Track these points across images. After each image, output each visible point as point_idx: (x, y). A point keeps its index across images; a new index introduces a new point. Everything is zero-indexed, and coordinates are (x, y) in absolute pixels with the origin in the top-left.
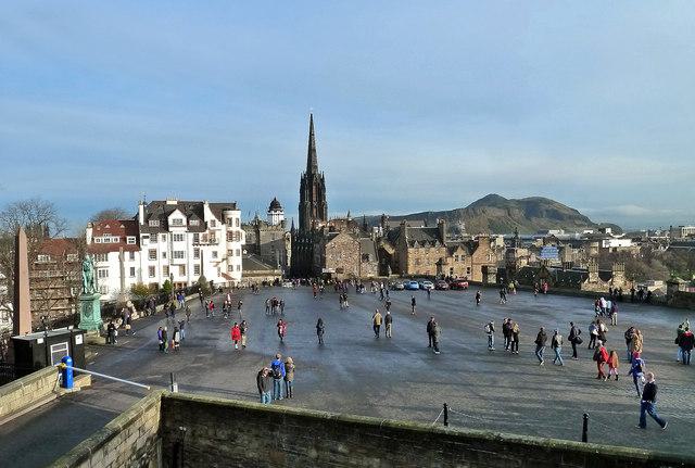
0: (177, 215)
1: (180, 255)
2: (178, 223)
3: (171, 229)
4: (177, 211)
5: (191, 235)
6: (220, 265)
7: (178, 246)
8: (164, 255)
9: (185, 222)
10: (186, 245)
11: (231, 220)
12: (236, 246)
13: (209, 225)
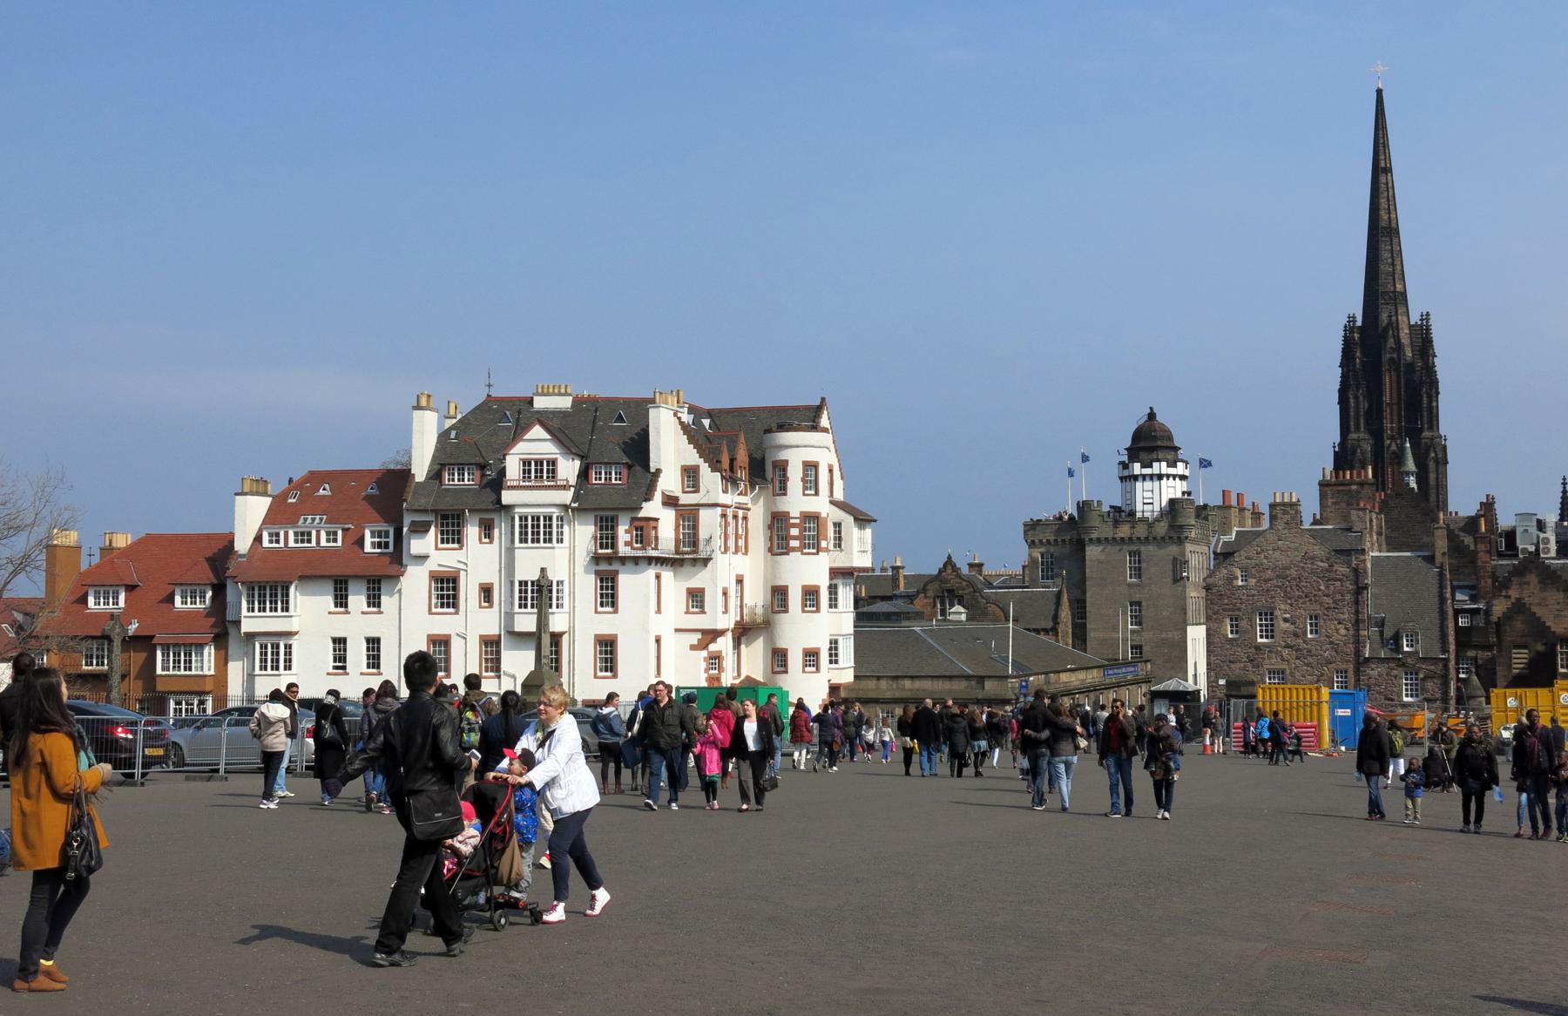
0: (537, 443)
2: (538, 471)
8: (487, 592)
10: (568, 557)
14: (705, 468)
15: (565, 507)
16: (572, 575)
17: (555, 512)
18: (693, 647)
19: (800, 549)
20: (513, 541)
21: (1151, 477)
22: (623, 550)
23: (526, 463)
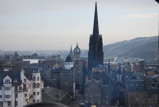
0: (7, 78)
1: (8, 96)
2: (7, 81)
3: (4, 85)
4: (7, 76)
5: (13, 88)
6: (28, 100)
7: (7, 93)
9: (11, 81)
10: (11, 92)
11: (35, 77)
12: (38, 90)
13: (23, 81)
14: (27, 79)
15: (11, 86)
16: (12, 94)
17: (10, 86)
18: (25, 101)
19: (37, 88)
20: (4, 90)
21: (69, 64)
22: (18, 91)
23: (6, 80)
